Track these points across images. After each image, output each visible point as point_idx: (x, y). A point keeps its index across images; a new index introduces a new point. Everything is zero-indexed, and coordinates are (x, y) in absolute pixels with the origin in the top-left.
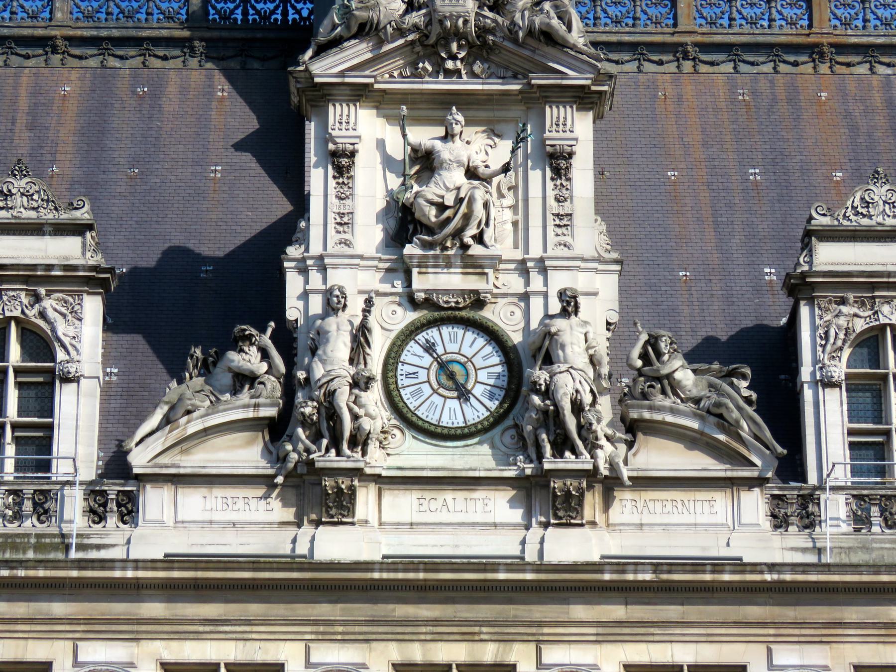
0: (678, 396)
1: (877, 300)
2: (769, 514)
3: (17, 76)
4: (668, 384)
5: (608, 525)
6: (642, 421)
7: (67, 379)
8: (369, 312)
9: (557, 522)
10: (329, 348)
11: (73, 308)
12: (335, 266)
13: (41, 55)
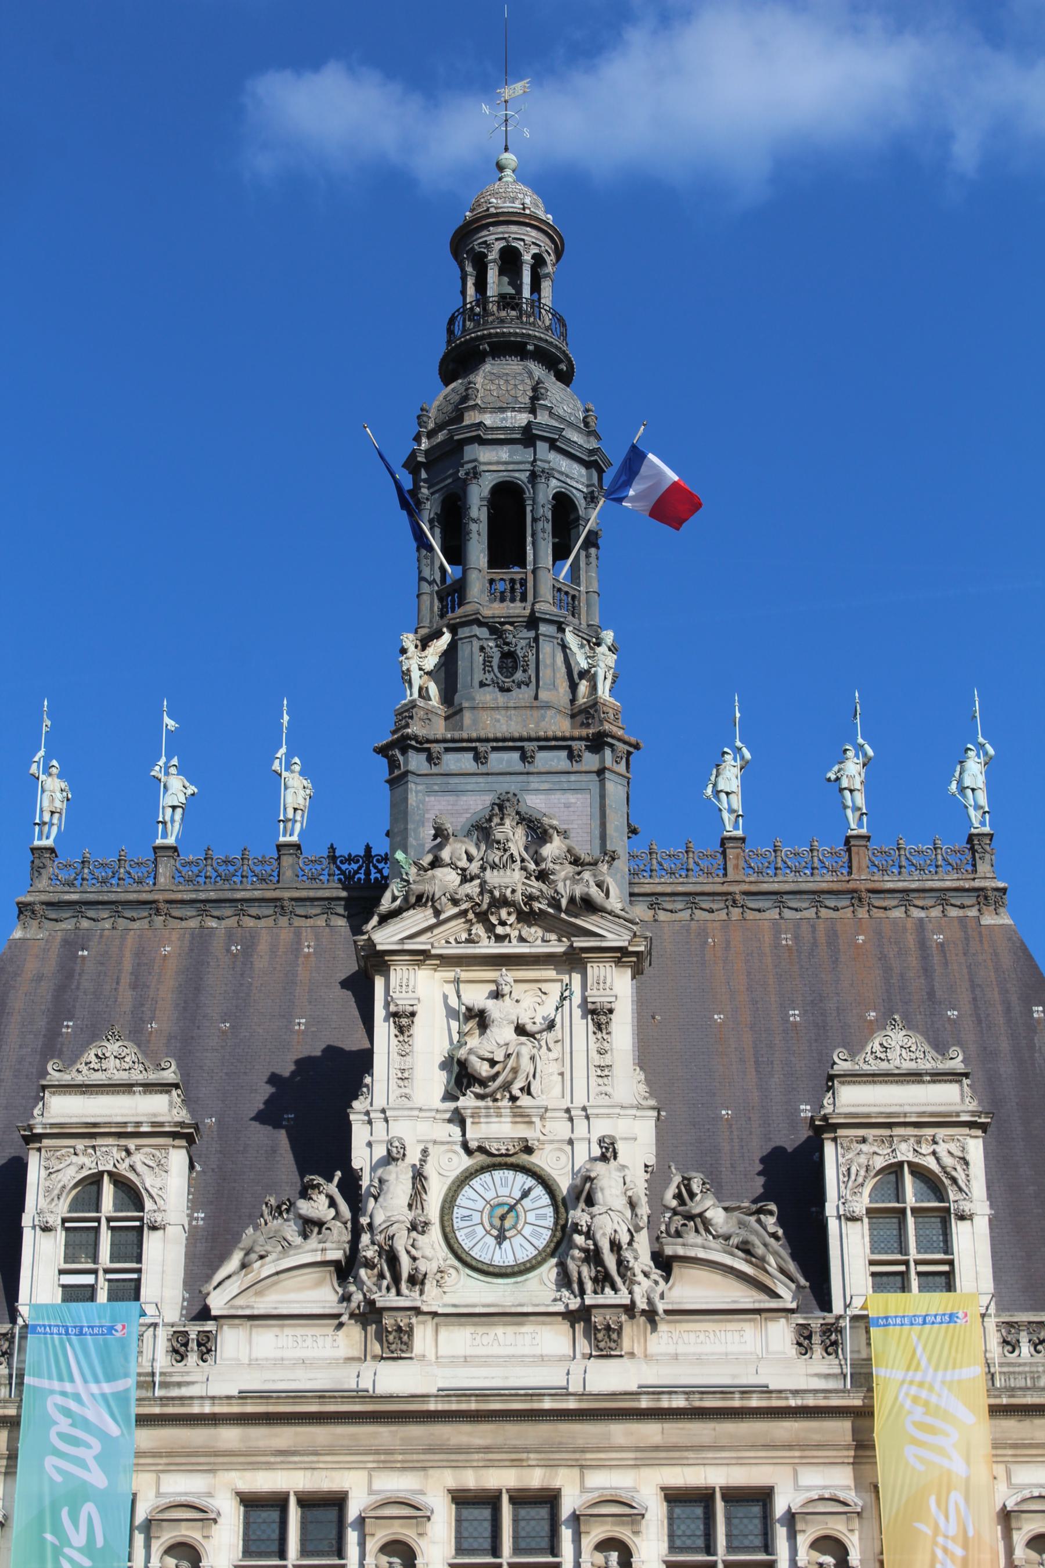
0: (711, 1233)
1: (895, 1139)
2: (795, 1342)
3: (123, 938)
5: (646, 1356)
7: (154, 1228)
8: (424, 1161)
10: (390, 1196)
12: (396, 1119)
13: (145, 918)
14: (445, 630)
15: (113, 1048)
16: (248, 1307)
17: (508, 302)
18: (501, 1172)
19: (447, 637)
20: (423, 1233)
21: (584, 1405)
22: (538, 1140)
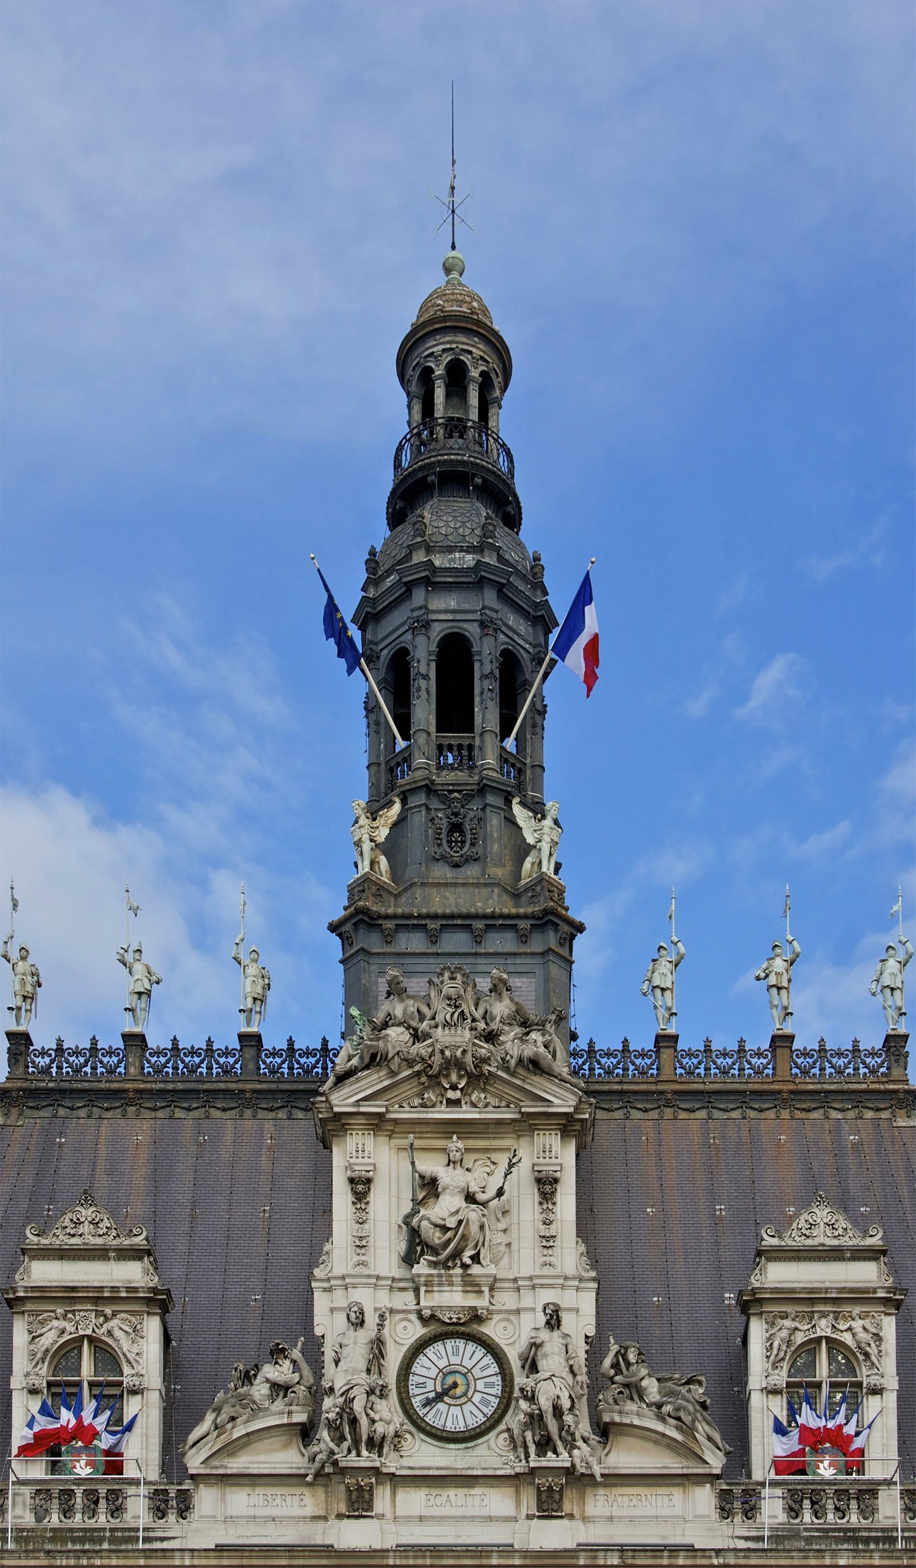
4: (634, 1391)
6: (613, 1423)
9: (541, 1514)
11: (135, 1327)
14: (397, 800)
16: (222, 1466)
18: (453, 1341)
20: (381, 1396)
21: (528, 1562)
22: (488, 1310)
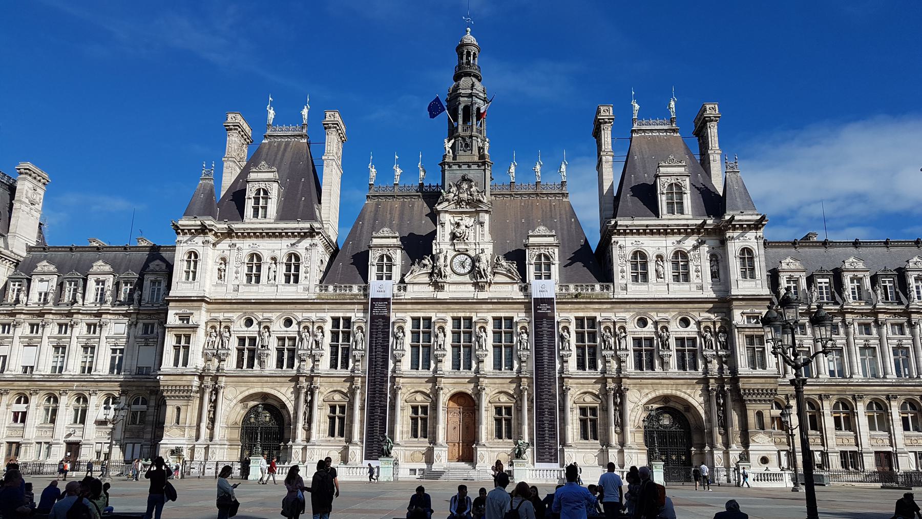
15: (385, 229)
17: (468, 63)
19: (453, 141)
